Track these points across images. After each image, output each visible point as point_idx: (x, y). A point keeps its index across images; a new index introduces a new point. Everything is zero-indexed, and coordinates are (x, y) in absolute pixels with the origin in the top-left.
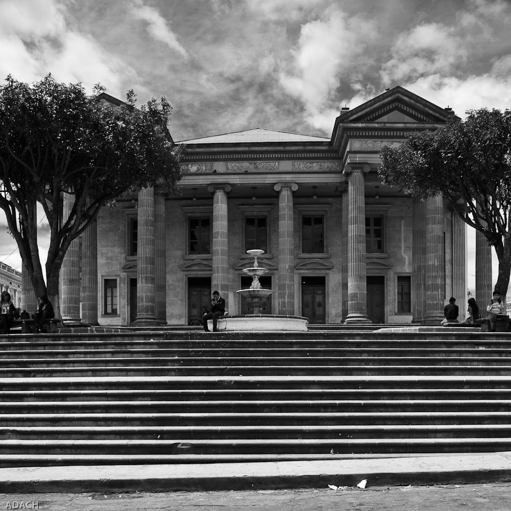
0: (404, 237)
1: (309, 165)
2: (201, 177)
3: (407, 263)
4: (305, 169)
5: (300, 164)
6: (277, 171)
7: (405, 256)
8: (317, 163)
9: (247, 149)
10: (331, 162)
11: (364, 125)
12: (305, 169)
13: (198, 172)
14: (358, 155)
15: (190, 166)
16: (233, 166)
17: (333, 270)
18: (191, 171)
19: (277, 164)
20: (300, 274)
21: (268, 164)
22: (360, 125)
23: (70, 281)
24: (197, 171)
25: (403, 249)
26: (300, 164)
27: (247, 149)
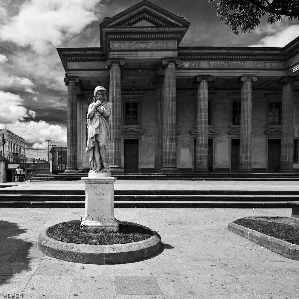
1: (264, 64)
2: (192, 71)
4: (261, 67)
8: (269, 63)
9: (226, 51)
10: (278, 63)
12: (261, 67)
13: (190, 67)
15: (184, 63)
16: (213, 64)
18: (185, 66)
19: (243, 63)
20: (231, 137)
21: (237, 63)
23: (116, 139)
24: (189, 67)
26: (258, 63)
27: (226, 51)
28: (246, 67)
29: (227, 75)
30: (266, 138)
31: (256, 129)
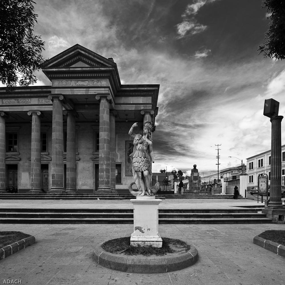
0: (118, 143)
3: (119, 157)
5: (42, 100)
6: (30, 104)
7: (118, 154)
11: (57, 70)
12: (45, 103)
14: (56, 90)
17: (80, 161)
19: (30, 100)
22: (54, 70)
25: (117, 150)
26: (42, 100)
28: (32, 103)
29: (17, 111)
30: (93, 163)
31: (85, 155)
